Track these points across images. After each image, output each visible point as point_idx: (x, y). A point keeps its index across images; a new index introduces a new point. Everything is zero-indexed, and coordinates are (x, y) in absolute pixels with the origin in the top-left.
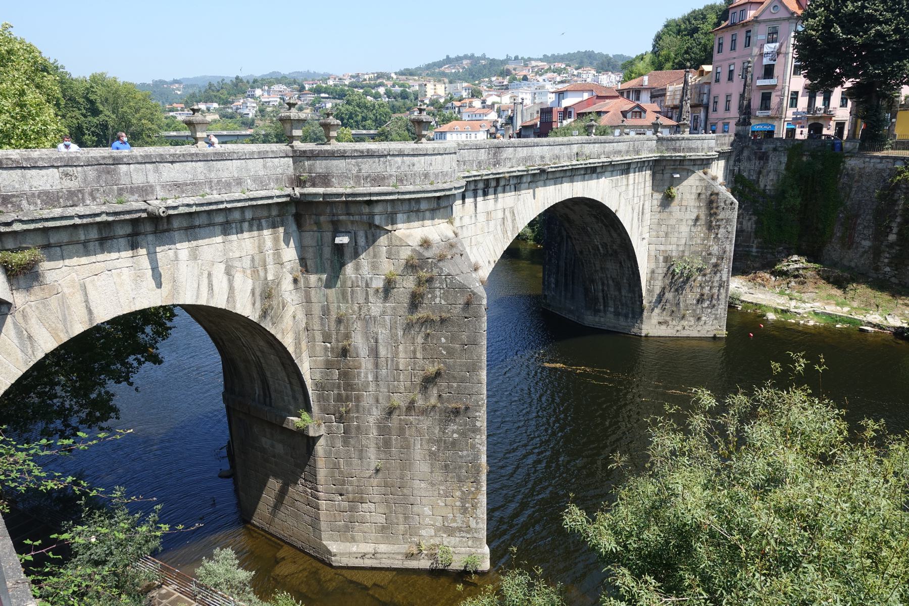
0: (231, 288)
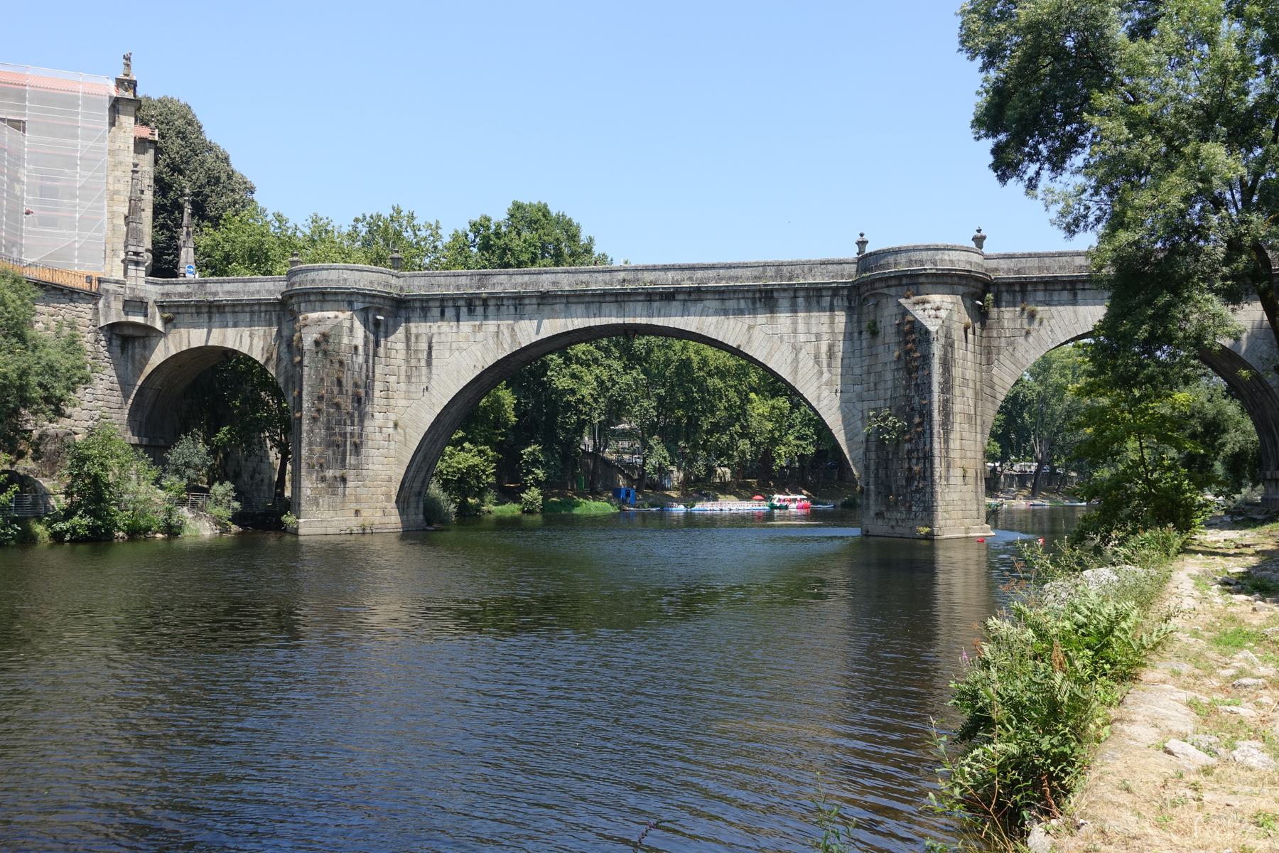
0: (251, 344)
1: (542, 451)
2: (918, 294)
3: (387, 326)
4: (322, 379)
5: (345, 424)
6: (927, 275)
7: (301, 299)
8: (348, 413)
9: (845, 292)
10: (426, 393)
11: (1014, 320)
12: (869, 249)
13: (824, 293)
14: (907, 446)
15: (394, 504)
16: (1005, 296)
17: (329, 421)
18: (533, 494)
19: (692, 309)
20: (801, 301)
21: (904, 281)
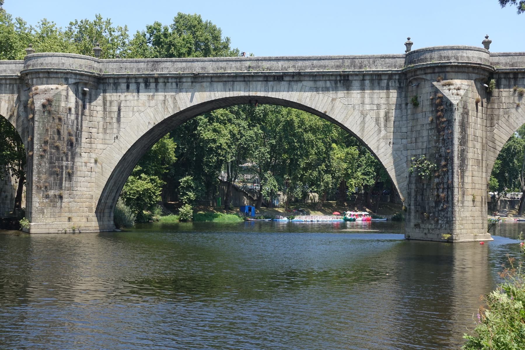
1: (193, 180)
2: (445, 79)
3: (90, 95)
4: (47, 130)
5: (62, 160)
6: (452, 67)
7: (34, 76)
8: (64, 153)
9: (397, 77)
10: (116, 140)
11: (509, 97)
12: (413, 48)
13: (383, 77)
14: (436, 180)
15: (94, 214)
16: (504, 82)
17: (51, 158)
18: (186, 209)
19: (295, 87)
20: (367, 82)
21: (437, 70)
